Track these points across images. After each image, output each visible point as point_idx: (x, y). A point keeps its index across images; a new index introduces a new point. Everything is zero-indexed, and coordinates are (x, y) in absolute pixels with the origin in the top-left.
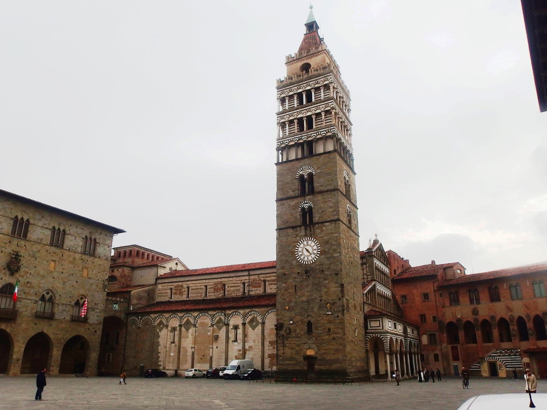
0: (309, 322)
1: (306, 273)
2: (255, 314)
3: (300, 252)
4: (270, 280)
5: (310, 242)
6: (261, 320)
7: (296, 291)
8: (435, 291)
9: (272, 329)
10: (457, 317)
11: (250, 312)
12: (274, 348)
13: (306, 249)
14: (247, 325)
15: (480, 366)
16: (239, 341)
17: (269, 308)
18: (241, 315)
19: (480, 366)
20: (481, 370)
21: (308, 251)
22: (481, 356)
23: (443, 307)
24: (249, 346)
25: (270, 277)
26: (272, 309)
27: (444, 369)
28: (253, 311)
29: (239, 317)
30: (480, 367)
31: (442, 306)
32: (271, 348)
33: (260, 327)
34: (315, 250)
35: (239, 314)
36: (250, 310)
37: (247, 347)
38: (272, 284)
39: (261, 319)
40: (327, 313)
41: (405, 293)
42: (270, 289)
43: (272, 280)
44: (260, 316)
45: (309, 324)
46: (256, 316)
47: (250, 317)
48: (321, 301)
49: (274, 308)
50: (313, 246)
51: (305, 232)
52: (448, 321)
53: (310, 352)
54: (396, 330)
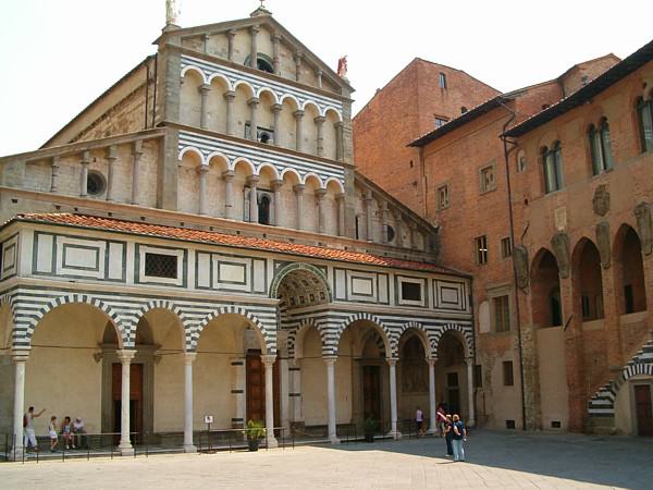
8: (507, 154)
10: (555, 229)
15: (612, 397)
19: (612, 397)
20: (613, 415)
22: (613, 363)
23: (526, 202)
27: (524, 408)
30: (612, 401)
31: (523, 201)
41: (442, 180)
52: (536, 248)
54: (178, 281)
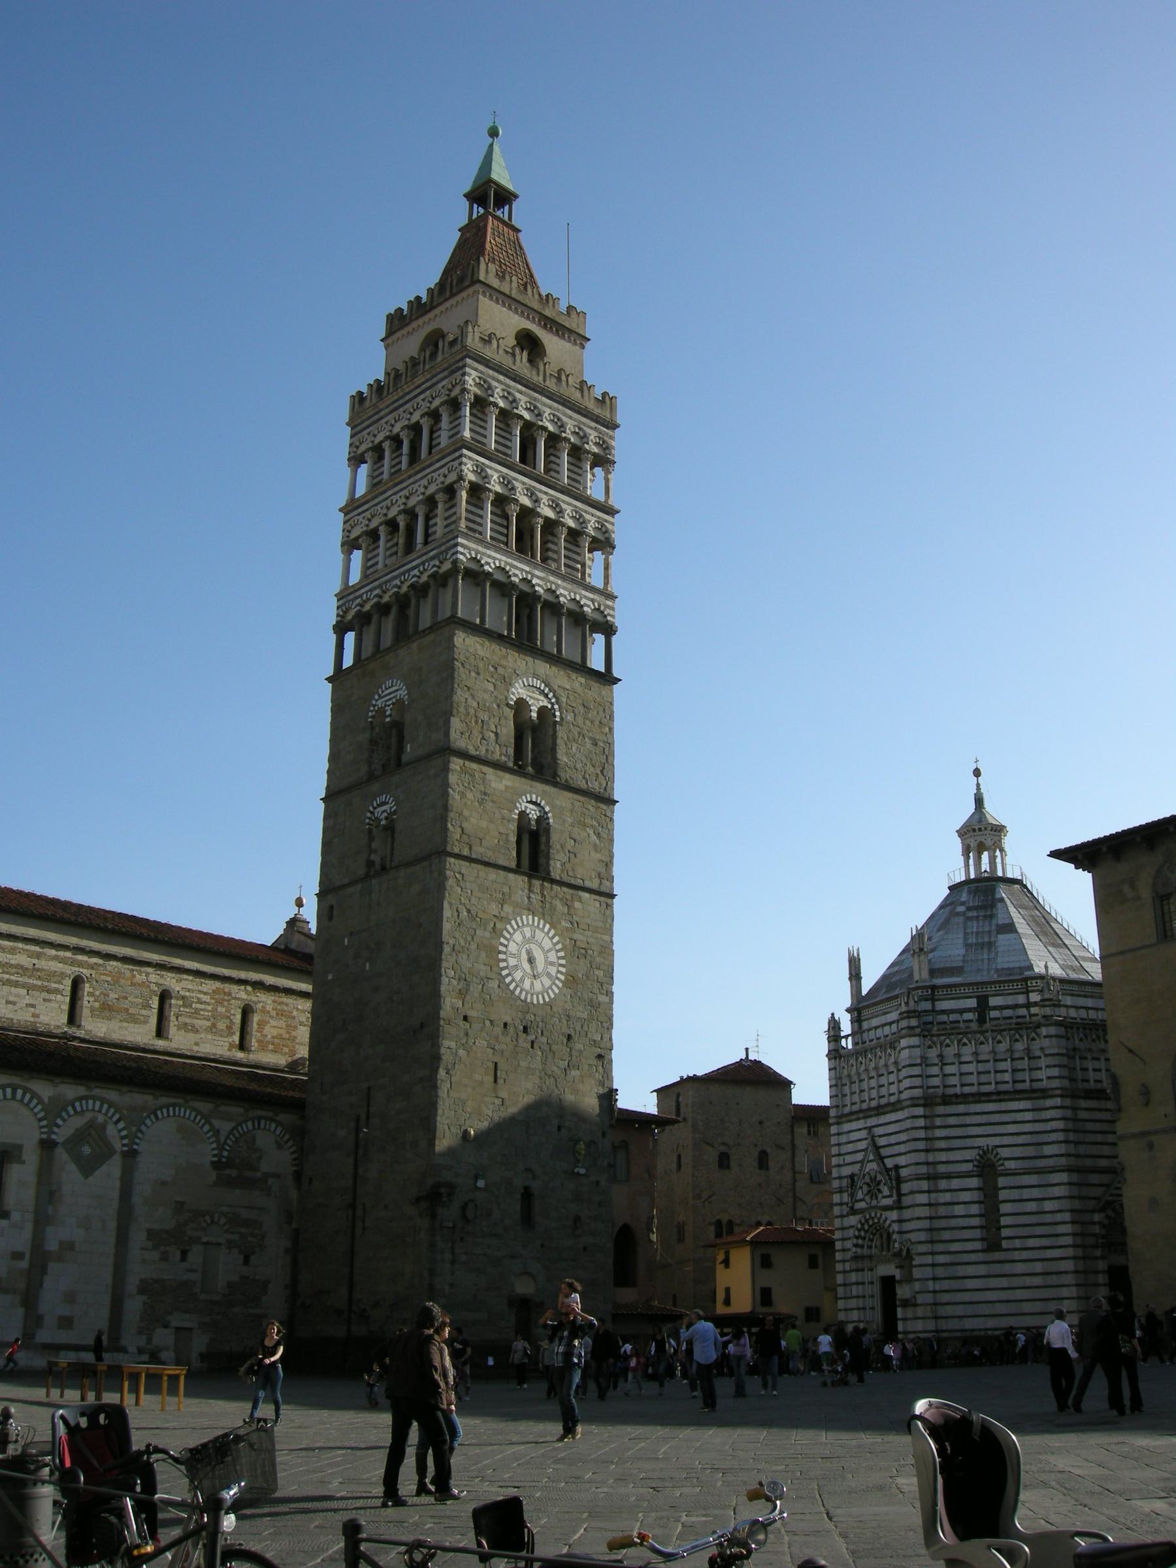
0: (526, 1188)
1: (525, 1030)
2: (100, 1111)
3: (513, 955)
4: (12, 966)
5: (539, 935)
6: (126, 1141)
7: (495, 1081)
9: (164, 1183)
11: (80, 1099)
12: (165, 1258)
13: (529, 952)
14: (61, 1154)
16: (15, 1216)
17: (164, 1100)
18: (39, 1107)
21: (531, 961)
24: (61, 1243)
25: (13, 951)
26: (174, 1105)
28: (94, 1098)
29: (24, 1111)
32: (155, 1255)
33: (113, 1169)
34: (552, 964)
35: (30, 1100)
36: (81, 1091)
37: (52, 1245)
38: (16, 984)
39: (123, 1138)
40: (576, 1170)
42: (8, 1002)
43: (22, 967)
44: (121, 1125)
45: (527, 1195)
46: (101, 1119)
47: (77, 1122)
48: (559, 1128)
49: (180, 1101)
50: (549, 951)
51: (529, 898)
53: (524, 1288)
